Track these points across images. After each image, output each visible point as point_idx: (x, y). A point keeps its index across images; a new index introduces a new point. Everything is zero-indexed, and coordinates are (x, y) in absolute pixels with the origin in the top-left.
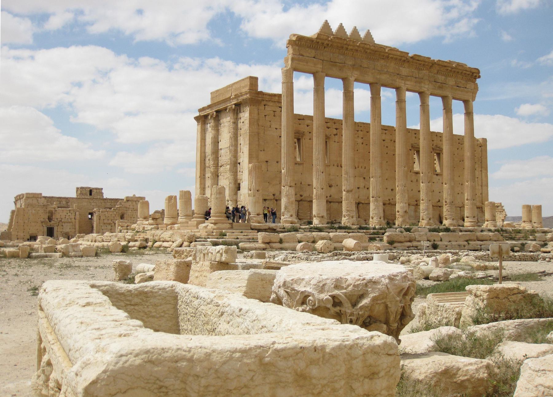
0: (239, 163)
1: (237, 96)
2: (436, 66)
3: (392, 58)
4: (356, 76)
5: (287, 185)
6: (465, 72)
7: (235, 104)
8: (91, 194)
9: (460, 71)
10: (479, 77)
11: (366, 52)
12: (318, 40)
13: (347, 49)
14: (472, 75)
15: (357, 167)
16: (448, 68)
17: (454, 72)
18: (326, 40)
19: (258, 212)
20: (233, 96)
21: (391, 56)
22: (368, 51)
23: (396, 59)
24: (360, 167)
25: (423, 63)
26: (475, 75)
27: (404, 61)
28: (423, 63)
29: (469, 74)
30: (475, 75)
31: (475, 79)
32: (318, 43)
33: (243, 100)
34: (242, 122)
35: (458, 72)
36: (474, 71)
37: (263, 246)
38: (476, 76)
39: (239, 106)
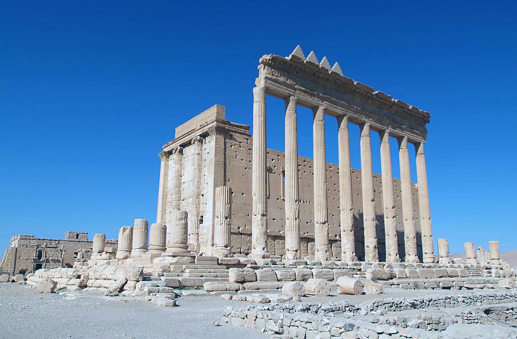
0: (203, 195)
1: (202, 127)
2: (395, 106)
3: (358, 93)
4: (326, 105)
5: (259, 214)
7: (200, 135)
8: (77, 238)
9: (415, 114)
10: (429, 122)
11: (336, 83)
12: (291, 63)
16: (404, 110)
17: (409, 114)
20: (199, 127)
21: (358, 90)
22: (338, 82)
26: (426, 119)
27: (369, 97)
29: (420, 118)
30: (426, 119)
31: (425, 123)
33: (209, 128)
34: (207, 152)
35: (412, 115)
36: (425, 115)
37: (237, 286)
38: (426, 120)
39: (204, 135)
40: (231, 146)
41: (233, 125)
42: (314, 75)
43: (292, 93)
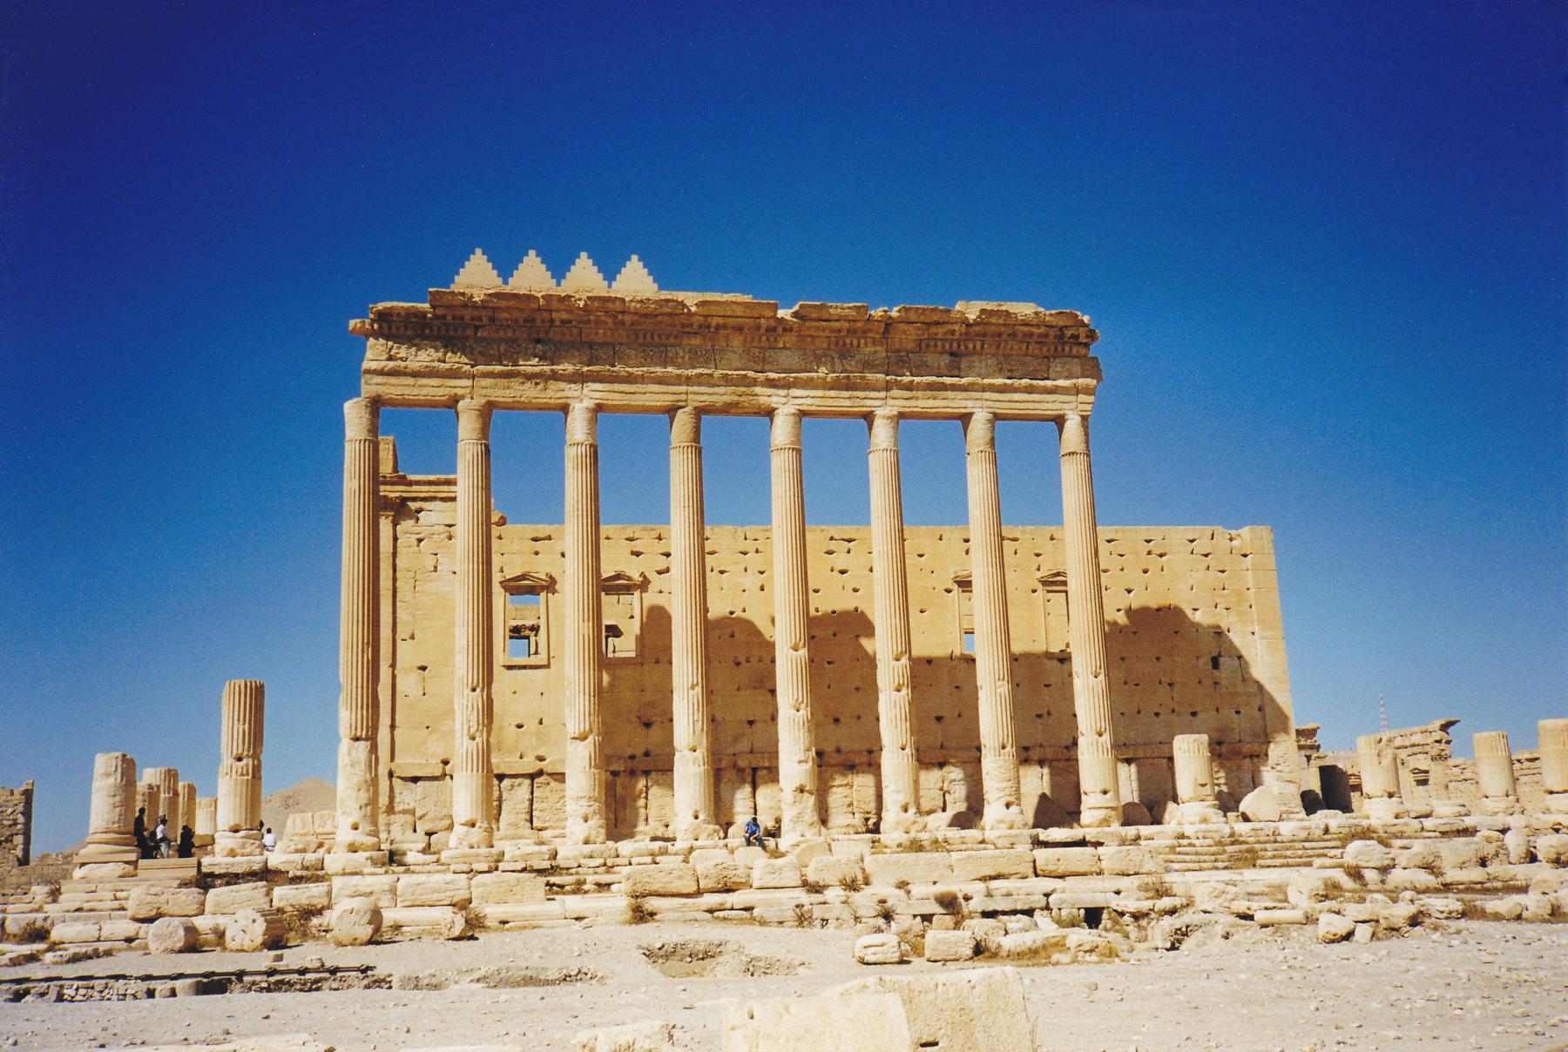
2: (902, 326)
4: (598, 395)
6: (1026, 329)
12: (440, 312)
13: (552, 321)
14: (1062, 336)
15: (742, 659)
18: (465, 306)
19: (232, 823)
21: (714, 321)
22: (628, 318)
23: (740, 329)
24: (754, 660)
25: (846, 325)
28: (846, 325)
29: (1046, 335)
30: (1069, 333)
32: (444, 317)
40: (420, 541)
41: (418, 483)
42: (534, 321)
43: (460, 392)
